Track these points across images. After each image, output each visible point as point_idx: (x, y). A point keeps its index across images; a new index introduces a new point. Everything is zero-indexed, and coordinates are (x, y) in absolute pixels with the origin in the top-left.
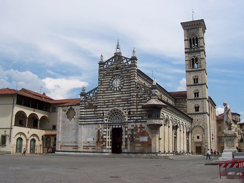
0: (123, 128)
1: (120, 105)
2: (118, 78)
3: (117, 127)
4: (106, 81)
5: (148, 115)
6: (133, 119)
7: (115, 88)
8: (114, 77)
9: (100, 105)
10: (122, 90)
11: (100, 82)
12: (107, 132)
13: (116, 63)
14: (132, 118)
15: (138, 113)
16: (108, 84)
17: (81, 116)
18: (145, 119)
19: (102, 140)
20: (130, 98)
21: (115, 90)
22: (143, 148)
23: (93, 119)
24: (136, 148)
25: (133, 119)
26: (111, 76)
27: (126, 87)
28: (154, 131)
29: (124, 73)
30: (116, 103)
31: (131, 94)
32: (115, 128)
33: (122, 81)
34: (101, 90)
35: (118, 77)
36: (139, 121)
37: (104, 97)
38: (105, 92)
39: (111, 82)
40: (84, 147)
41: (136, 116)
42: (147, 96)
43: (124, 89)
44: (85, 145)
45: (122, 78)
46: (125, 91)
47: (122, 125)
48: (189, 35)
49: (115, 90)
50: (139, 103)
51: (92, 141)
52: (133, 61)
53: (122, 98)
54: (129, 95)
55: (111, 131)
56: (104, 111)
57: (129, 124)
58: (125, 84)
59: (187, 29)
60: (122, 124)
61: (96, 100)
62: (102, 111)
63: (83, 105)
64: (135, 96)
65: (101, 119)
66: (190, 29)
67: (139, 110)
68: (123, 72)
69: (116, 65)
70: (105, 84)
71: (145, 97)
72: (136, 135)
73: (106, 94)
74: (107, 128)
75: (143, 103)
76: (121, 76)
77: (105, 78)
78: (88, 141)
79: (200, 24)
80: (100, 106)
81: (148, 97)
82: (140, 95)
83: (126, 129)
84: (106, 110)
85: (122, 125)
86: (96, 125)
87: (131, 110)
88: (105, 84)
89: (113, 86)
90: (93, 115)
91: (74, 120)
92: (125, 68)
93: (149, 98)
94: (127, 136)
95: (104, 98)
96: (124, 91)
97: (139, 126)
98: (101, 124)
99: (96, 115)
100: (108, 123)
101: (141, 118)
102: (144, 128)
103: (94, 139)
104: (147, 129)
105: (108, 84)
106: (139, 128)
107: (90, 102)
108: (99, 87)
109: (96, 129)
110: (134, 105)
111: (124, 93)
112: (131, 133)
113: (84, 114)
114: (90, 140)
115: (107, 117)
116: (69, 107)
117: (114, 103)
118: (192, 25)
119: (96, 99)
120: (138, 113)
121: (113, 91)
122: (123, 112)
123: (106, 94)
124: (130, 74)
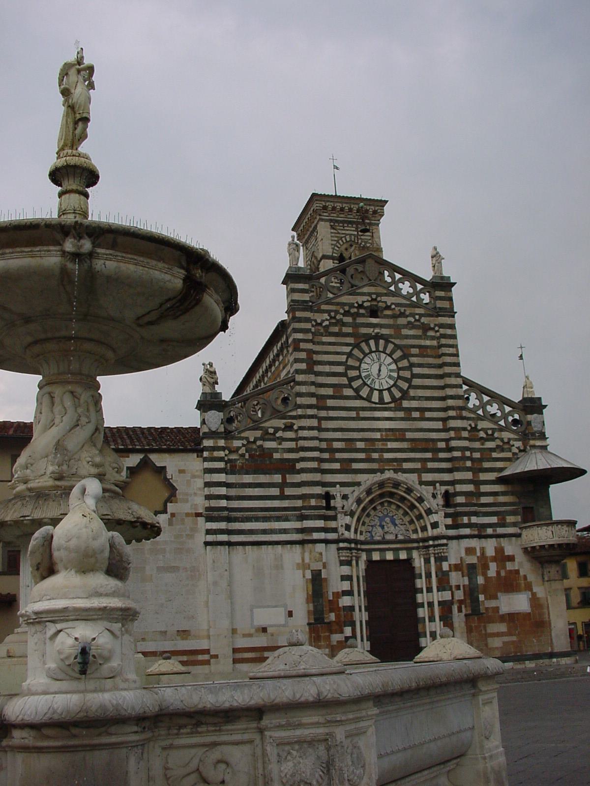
0: (418, 562)
1: (406, 465)
2: (381, 349)
3: (390, 556)
4: (326, 358)
5: (520, 510)
6: (470, 525)
7: (372, 390)
8: (363, 345)
9: (313, 459)
10: (406, 404)
11: (303, 355)
12: (355, 579)
13: (372, 289)
14: (465, 520)
15: (484, 500)
16: (341, 369)
17: (214, 503)
18: (514, 524)
19: (332, 617)
20: (447, 441)
21: (375, 397)
22: (514, 638)
23: (278, 519)
24: (490, 640)
25: (470, 525)
26: (351, 340)
27: (420, 393)
28: (553, 570)
29: (407, 337)
30: (387, 456)
31: (453, 424)
32: (383, 562)
33: (400, 365)
34: (312, 395)
35: (385, 348)
36: (490, 531)
37: (325, 424)
38: (330, 403)
39: (351, 362)
40: (239, 656)
41: (476, 514)
42: (512, 436)
43: (414, 398)
44: (242, 643)
45: (398, 354)
46: (422, 410)
47: (414, 548)
48: (338, 241)
49: (375, 397)
50: (481, 460)
51: (283, 622)
52: (440, 293)
53: (409, 435)
54: (439, 425)
55: (364, 574)
56: (333, 485)
57: (450, 542)
58: (416, 382)
59: (331, 221)
60: (410, 545)
61: (290, 434)
62: (324, 484)
63: (222, 454)
64: (465, 434)
65: (320, 523)
66: (343, 222)
67: (484, 488)
68: (405, 332)
69: (370, 294)
70: (327, 369)
71: (506, 440)
72: (485, 590)
73: (332, 414)
74: (354, 562)
75: (499, 465)
76: (397, 347)
77: (324, 344)
78: (260, 621)
79: (375, 212)
80: (314, 465)
81: (516, 440)
82: (485, 430)
83: (445, 566)
84: (343, 484)
85: (414, 548)
86: (298, 548)
87: (459, 488)
88: (327, 369)
89: (365, 384)
90: (276, 504)
91: (170, 523)
92: (413, 315)
93: (519, 444)
94: (446, 596)
95: (327, 430)
96: (416, 409)
97: (490, 552)
98: (326, 542)
99: (299, 503)
100: (356, 542)
101: (494, 520)
102: (511, 558)
103: (290, 614)
104: (523, 565)
105: (341, 369)
106: (494, 559)
107: (259, 443)
108: (300, 378)
109: (303, 566)
110: (468, 469)
111: (416, 414)
112: (466, 581)
113: (227, 498)
114: (271, 617)
115: (352, 514)
116: (134, 460)
117: (375, 456)
118: (350, 210)
119: (289, 428)
120: (484, 500)
121: (366, 404)
122: (424, 493)
123: (332, 414)
124: (435, 343)
